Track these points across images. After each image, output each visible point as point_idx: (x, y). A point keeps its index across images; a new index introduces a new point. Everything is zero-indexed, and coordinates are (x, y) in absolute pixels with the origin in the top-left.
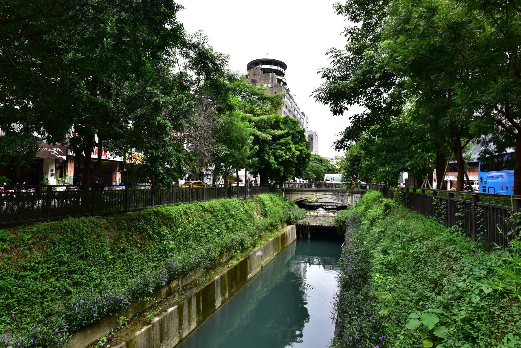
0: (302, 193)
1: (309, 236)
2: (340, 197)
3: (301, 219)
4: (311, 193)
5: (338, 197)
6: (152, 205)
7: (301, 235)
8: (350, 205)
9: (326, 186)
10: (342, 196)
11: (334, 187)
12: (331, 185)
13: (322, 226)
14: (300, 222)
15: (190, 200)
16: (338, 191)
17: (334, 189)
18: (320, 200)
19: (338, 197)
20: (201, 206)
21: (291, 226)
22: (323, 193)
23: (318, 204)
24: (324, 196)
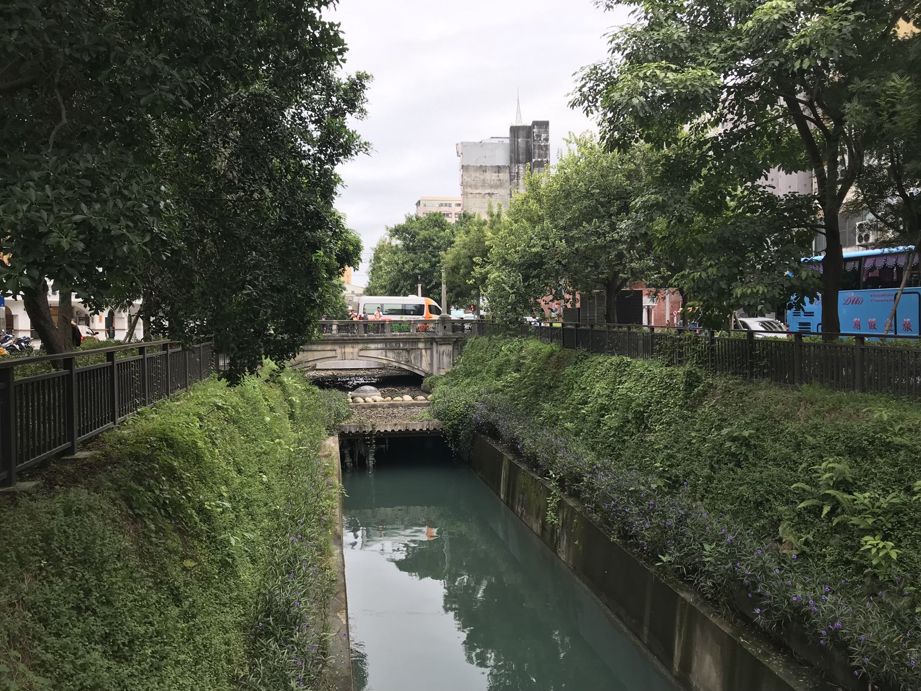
1: (371, 460)
2: (404, 353)
3: (348, 417)
4: (329, 347)
6: (113, 420)
7: (348, 460)
8: (428, 375)
9: (366, 325)
10: (408, 351)
11: (387, 330)
12: (380, 326)
13: (407, 430)
14: (350, 425)
15: (168, 389)
16: (398, 341)
17: (388, 335)
18: (319, 365)
19: (399, 354)
20: (219, 408)
21: (332, 438)
22: (360, 346)
23: (323, 374)
24: (362, 353)
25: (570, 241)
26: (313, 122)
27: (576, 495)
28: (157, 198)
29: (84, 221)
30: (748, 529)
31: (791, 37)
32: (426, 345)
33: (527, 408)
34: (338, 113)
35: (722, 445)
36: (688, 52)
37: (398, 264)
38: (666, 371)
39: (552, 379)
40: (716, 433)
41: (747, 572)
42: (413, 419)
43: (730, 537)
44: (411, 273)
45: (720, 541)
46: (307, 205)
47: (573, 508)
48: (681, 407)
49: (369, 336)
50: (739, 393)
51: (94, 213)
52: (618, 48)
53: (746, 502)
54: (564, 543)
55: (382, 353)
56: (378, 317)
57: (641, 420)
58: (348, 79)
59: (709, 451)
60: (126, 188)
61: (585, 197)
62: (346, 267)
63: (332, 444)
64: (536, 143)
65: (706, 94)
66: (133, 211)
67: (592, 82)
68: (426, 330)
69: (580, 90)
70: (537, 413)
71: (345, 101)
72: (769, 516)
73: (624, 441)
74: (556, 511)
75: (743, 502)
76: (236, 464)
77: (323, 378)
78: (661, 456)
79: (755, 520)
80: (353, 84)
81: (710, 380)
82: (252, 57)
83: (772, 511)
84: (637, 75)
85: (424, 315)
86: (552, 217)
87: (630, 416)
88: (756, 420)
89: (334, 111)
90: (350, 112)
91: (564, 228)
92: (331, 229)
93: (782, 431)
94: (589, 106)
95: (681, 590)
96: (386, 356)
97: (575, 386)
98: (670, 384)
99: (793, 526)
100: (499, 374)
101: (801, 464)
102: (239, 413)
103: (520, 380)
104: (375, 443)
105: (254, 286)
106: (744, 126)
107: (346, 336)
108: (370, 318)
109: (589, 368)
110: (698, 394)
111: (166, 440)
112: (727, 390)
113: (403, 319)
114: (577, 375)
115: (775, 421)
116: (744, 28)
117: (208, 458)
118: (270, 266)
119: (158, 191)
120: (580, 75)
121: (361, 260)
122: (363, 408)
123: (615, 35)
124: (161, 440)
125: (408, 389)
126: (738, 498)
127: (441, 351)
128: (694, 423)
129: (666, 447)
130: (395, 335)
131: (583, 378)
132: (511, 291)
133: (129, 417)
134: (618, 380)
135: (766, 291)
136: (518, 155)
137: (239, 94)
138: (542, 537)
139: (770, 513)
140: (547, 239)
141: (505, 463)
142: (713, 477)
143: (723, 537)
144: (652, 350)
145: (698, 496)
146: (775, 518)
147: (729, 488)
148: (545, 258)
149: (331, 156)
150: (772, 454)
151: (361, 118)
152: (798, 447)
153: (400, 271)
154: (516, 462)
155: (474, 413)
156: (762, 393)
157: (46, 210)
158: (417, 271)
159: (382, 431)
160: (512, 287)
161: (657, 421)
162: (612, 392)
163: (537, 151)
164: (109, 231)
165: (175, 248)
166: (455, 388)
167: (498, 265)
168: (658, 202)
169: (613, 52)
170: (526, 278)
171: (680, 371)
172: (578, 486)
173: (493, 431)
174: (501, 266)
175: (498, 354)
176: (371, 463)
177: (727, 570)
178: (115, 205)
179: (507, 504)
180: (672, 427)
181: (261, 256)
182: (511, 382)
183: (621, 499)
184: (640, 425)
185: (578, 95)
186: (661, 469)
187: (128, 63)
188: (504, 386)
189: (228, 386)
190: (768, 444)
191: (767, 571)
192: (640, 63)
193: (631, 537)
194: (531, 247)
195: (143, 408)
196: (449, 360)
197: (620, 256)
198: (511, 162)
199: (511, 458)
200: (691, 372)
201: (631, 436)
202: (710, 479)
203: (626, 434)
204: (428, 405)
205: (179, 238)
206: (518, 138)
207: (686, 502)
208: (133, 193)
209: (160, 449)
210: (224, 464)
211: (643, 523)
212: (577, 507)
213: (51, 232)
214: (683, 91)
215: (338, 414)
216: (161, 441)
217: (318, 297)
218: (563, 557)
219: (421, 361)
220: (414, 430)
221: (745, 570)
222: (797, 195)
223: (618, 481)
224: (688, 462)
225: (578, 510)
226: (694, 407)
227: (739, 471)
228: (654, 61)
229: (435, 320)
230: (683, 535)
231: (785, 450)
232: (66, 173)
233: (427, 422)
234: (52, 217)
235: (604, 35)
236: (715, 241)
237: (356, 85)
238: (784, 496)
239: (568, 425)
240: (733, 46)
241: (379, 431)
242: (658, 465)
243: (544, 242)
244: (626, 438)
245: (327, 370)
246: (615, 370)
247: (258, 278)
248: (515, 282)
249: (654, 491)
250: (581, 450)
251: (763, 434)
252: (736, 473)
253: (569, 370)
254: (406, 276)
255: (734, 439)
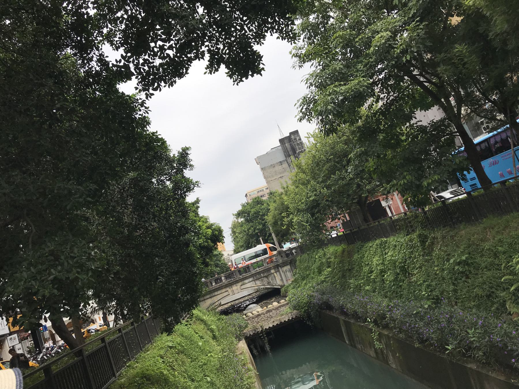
0: (212, 295)
1: (268, 347)
2: (265, 279)
3: (246, 327)
4: (224, 290)
5: (262, 280)
6: (114, 375)
7: (255, 351)
8: (282, 286)
9: (239, 271)
10: (266, 277)
12: (247, 269)
13: (281, 323)
14: (249, 331)
16: (259, 273)
17: (253, 272)
19: (262, 280)
20: (171, 347)
21: (241, 342)
22: (240, 284)
23: (226, 306)
24: (243, 287)
25: (328, 187)
26: (168, 180)
27: (386, 327)
28: (90, 251)
29: (55, 278)
30: (489, 313)
31: (395, 48)
32: (275, 270)
33: (342, 286)
34: (180, 171)
35: (454, 269)
36: (347, 73)
37: (245, 231)
38: (407, 238)
39: (349, 265)
40: (448, 264)
41: (498, 339)
42: (282, 315)
43: (480, 322)
44: (254, 233)
45: (476, 326)
46: (176, 224)
47: (388, 335)
48: (423, 255)
49: (243, 276)
50: (450, 237)
51: (59, 272)
52: (311, 85)
53: (481, 297)
54: (391, 357)
55: (253, 283)
56: (244, 264)
57: (405, 271)
58: (179, 153)
59: (448, 275)
60: (72, 252)
61: (327, 162)
62: (218, 244)
63: (243, 345)
64: (295, 143)
65: (365, 90)
66: (78, 263)
67: (306, 105)
68: (272, 262)
69: (301, 112)
70: (348, 287)
71: (180, 164)
72: (498, 301)
73: (401, 286)
74: (379, 340)
75: (480, 298)
76: (190, 377)
77: (226, 309)
78: (424, 287)
79: (491, 306)
80: (182, 155)
81: (433, 235)
82: (119, 164)
83: (498, 298)
84: (326, 94)
85: (269, 254)
86: (314, 178)
87: (398, 271)
88: (466, 249)
89: (176, 172)
90: (184, 169)
91: (322, 182)
92: (192, 231)
93: (483, 249)
94: (309, 118)
95: (467, 363)
96: (256, 284)
97: (363, 264)
98: (412, 245)
99: (513, 302)
100: (320, 272)
101: (502, 264)
102: (183, 346)
103: (332, 272)
104: (266, 337)
105: (163, 276)
106: (392, 98)
107: (231, 281)
108: (240, 266)
109: (366, 251)
110: (429, 245)
111: (145, 377)
112: (444, 237)
113: (258, 260)
114: (361, 258)
115: (477, 245)
116: (370, 52)
117: (171, 379)
118: (167, 262)
119: (89, 248)
120: (298, 104)
121: (224, 237)
122: (253, 318)
123: (307, 79)
124: (142, 378)
125: (274, 298)
126: (476, 297)
127: (285, 270)
128: (434, 262)
129: (424, 281)
130: (256, 271)
131: (365, 258)
132: (307, 225)
133: (123, 370)
134: (384, 252)
135: (439, 177)
136: (288, 152)
137: (125, 181)
138: (377, 358)
139: (497, 299)
140: (316, 191)
141: (342, 322)
142: (456, 289)
143: (476, 323)
144: (396, 230)
145: (453, 303)
146: (501, 301)
147: (468, 292)
148: (319, 201)
149: (181, 194)
150: (483, 265)
151: (192, 169)
152: (496, 256)
153: (248, 234)
154: (347, 319)
155: (314, 299)
156: (463, 232)
157: (33, 280)
158: (257, 231)
159: (268, 328)
160: (307, 222)
161: (414, 268)
162: (383, 261)
163: (297, 147)
164: (69, 278)
165: (115, 271)
166: (299, 289)
167: (296, 213)
168: (363, 152)
169: (310, 88)
170: (313, 215)
171: (415, 236)
172: (385, 321)
173: (328, 306)
174: (297, 213)
175: (315, 261)
176: (268, 349)
177: (487, 342)
178: (68, 263)
179: (351, 345)
180: (423, 269)
181: (162, 258)
182: (328, 275)
183: (412, 320)
184: (406, 273)
185: (301, 114)
186: (426, 295)
187: (56, 191)
188: (325, 278)
189: (167, 335)
190: (478, 260)
191: (509, 334)
192: (325, 88)
193: (426, 341)
194: (309, 198)
195: (130, 363)
196: (290, 274)
197: (359, 186)
198: (286, 157)
199: (343, 318)
200: (420, 234)
201: (403, 282)
202: (455, 291)
203: (400, 281)
204: (287, 304)
205: (116, 265)
206: (285, 144)
207: (448, 309)
208: (76, 254)
209: (143, 383)
210: (182, 380)
211: (429, 330)
212: (390, 333)
213: (39, 290)
214: (352, 93)
215: (240, 327)
216: (143, 379)
217: (197, 270)
218: (394, 366)
219: (275, 279)
220: (285, 321)
221: (497, 338)
222: (435, 121)
223: (406, 310)
224: (439, 286)
225: (391, 335)
226: (430, 253)
227: (469, 281)
228: (332, 84)
229: (275, 255)
230: (454, 329)
231: (490, 260)
232: (40, 257)
233: (290, 314)
234: (37, 282)
235: (302, 81)
236: (402, 161)
237: (184, 155)
238: (501, 287)
239: (367, 288)
240: (368, 62)
241: (266, 329)
242: (424, 293)
243: (315, 193)
244: (401, 284)
245: (228, 303)
246: (380, 248)
247: (163, 271)
248: (308, 219)
249: (428, 309)
250: (380, 299)
251: (474, 255)
252: (468, 283)
253: (356, 256)
254: (252, 236)
255: (459, 264)
